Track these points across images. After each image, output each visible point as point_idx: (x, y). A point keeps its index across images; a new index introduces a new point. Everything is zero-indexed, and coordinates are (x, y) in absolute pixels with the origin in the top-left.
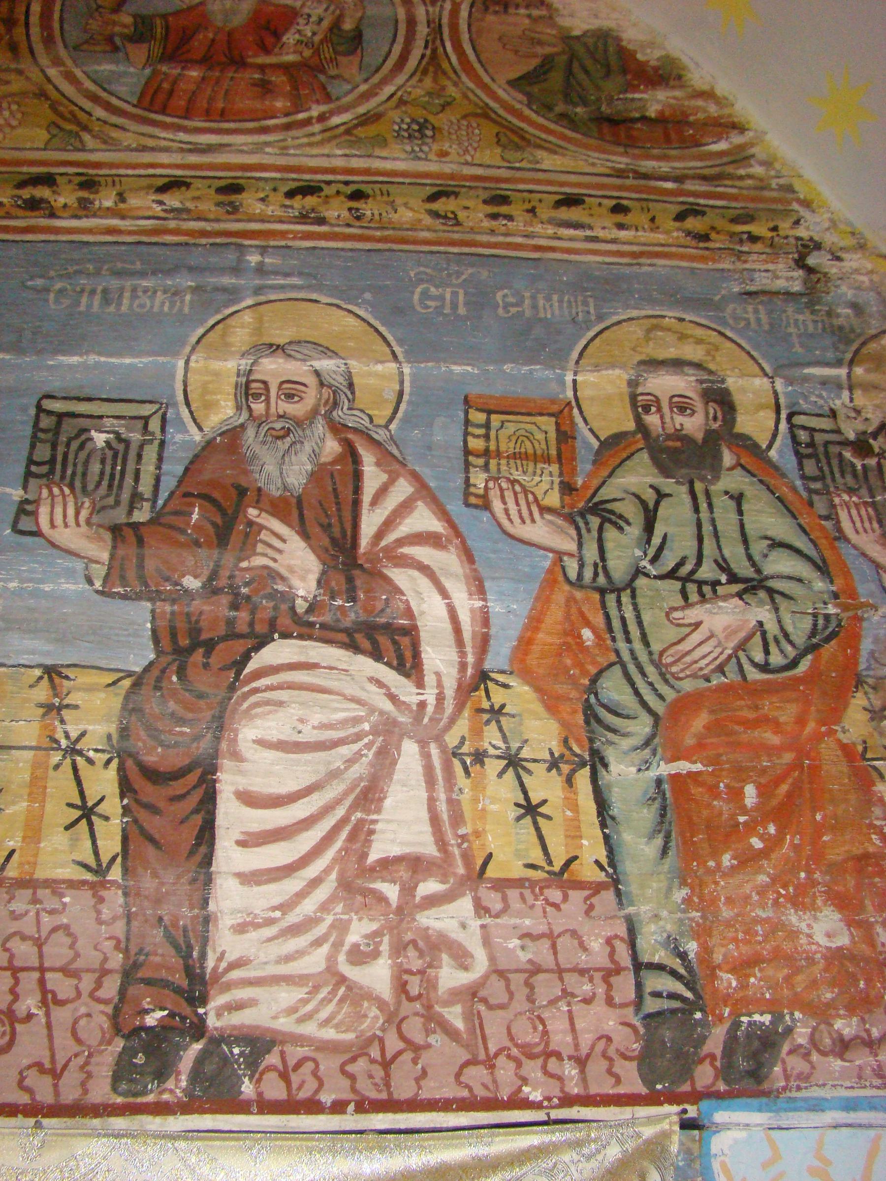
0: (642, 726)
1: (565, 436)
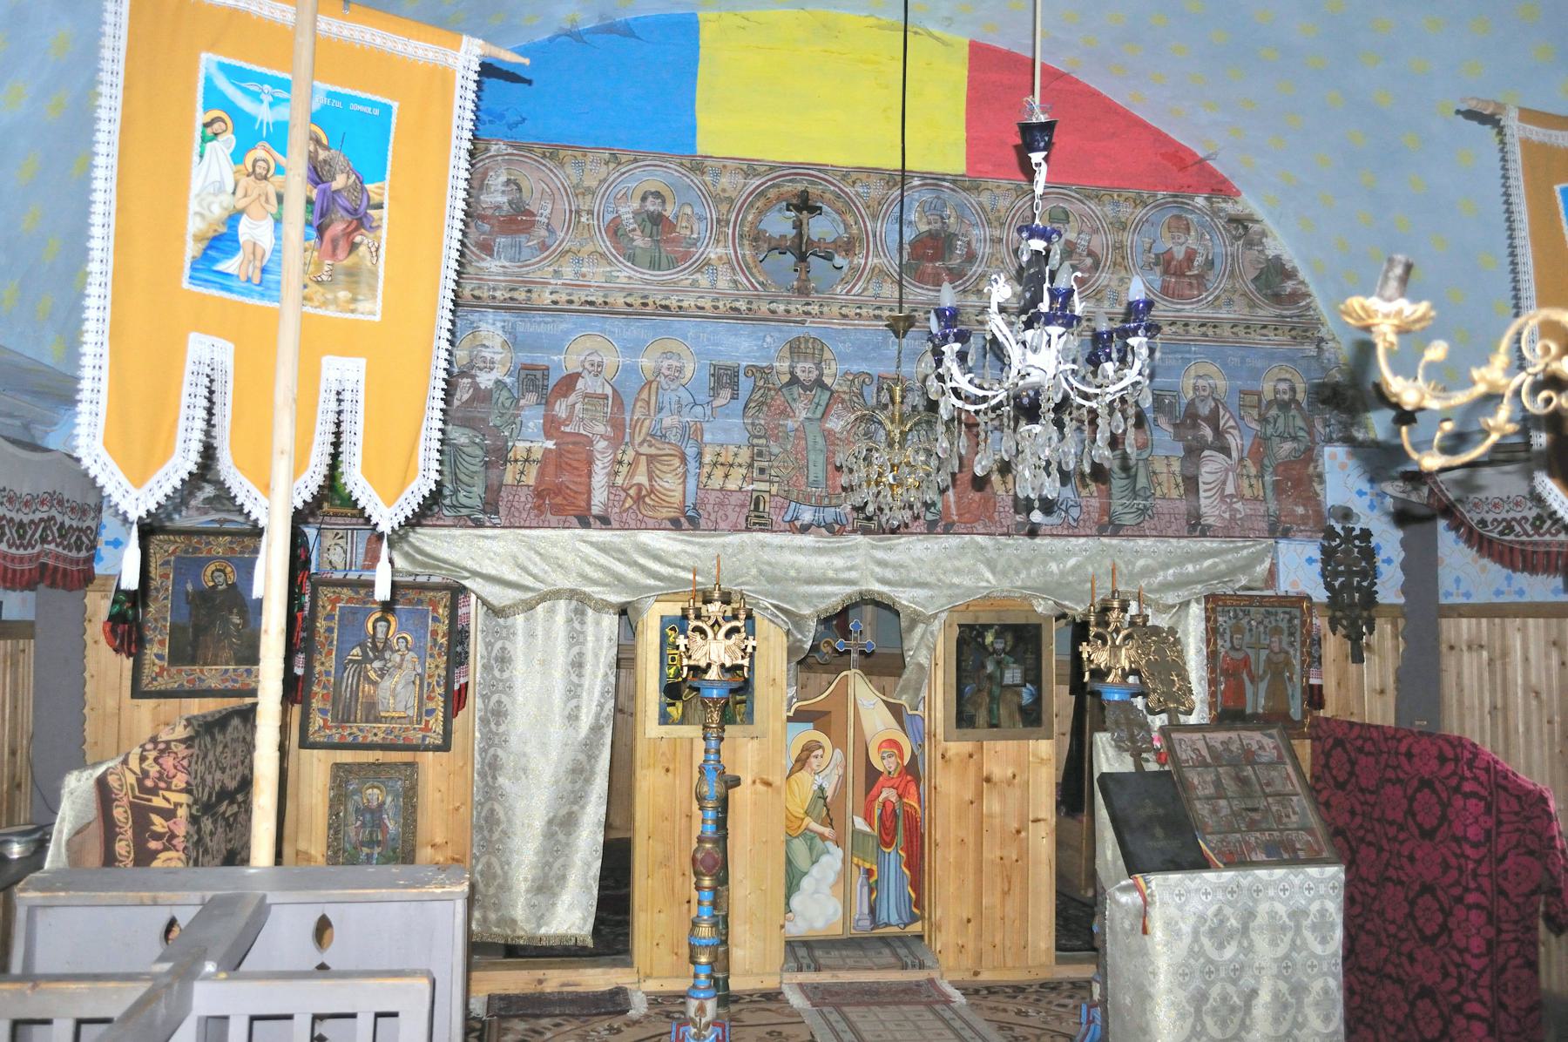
0: (1271, 469)
1: (1260, 401)
